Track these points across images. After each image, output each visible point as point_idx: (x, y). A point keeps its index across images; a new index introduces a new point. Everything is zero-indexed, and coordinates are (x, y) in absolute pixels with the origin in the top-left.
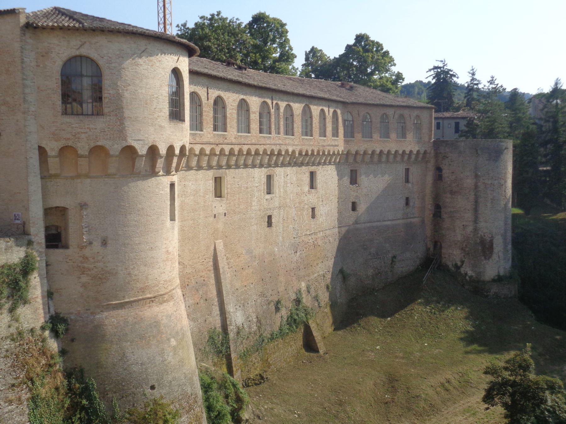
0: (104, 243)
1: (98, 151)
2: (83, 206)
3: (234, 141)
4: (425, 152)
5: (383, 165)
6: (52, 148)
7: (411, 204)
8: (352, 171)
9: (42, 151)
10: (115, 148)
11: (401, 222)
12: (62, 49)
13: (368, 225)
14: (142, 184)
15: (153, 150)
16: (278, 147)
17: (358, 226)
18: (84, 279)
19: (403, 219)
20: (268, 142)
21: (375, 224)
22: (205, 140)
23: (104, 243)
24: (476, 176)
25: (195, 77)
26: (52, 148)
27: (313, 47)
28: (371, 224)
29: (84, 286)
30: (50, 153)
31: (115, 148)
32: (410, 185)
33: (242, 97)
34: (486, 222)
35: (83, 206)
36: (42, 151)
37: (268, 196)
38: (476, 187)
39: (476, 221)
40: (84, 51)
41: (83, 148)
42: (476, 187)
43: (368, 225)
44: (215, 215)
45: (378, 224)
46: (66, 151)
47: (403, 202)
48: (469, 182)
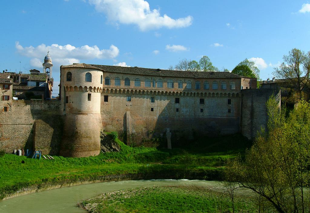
0: (73, 102)
1: (71, 87)
2: (70, 96)
3: (133, 88)
4: (237, 94)
6: (65, 86)
7: (231, 111)
9: (64, 87)
10: (73, 87)
11: (226, 117)
12: (67, 71)
13: (209, 117)
15: (81, 87)
18: (70, 108)
19: (227, 117)
20: (149, 89)
21: (211, 117)
22: (121, 87)
23: (73, 102)
24: (252, 102)
26: (65, 86)
28: (210, 117)
29: (70, 109)
30: (65, 87)
32: (231, 105)
35: (70, 96)
36: (64, 87)
38: (252, 105)
42: (252, 105)
43: (209, 117)
44: (127, 105)
45: (214, 117)
46: (67, 87)
47: (227, 111)
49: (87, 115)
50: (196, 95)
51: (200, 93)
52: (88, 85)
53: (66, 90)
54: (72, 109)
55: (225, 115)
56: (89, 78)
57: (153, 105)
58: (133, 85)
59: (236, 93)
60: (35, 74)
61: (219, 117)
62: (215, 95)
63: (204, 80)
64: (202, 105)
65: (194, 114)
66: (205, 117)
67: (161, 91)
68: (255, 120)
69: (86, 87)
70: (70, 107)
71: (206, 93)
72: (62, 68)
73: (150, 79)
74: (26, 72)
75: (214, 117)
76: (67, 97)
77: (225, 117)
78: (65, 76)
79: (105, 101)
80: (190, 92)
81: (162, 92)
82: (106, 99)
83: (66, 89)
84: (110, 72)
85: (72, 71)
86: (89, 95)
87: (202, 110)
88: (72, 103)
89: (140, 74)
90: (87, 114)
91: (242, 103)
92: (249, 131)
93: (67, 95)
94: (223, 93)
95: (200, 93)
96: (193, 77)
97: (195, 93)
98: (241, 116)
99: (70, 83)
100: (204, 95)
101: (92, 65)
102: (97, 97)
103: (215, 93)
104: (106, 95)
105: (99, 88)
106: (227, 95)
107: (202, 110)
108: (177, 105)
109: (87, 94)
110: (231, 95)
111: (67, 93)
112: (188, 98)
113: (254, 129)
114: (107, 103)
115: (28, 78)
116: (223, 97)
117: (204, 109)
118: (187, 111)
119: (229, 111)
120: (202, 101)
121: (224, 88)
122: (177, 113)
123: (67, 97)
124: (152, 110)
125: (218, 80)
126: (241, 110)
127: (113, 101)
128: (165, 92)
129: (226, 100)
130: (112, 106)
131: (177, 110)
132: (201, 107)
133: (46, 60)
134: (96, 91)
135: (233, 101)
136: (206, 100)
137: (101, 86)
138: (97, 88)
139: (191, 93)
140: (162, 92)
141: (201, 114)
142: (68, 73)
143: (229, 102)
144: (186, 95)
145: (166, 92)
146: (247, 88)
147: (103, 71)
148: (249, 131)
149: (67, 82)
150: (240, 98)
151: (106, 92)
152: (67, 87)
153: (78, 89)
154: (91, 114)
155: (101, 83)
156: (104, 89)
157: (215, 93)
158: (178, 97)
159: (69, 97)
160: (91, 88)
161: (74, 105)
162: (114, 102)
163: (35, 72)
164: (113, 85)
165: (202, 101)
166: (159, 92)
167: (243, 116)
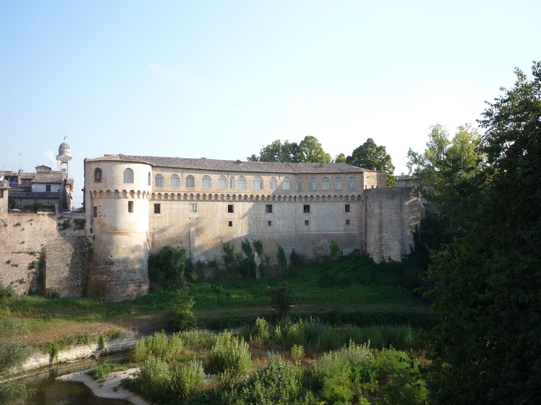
0: (104, 216)
1: (101, 192)
4: (359, 196)
5: (328, 203)
7: (351, 223)
8: (305, 206)
10: (105, 191)
11: (343, 232)
12: (94, 167)
14: (119, 200)
15: (117, 191)
16: (233, 194)
17: (309, 233)
21: (322, 233)
22: (180, 190)
23: (104, 216)
24: (381, 208)
25: (155, 168)
27: (370, 143)
31: (105, 191)
32: (349, 213)
33: (189, 174)
34: (387, 233)
37: (230, 214)
38: (381, 213)
39: (381, 231)
40: (98, 167)
41: (98, 191)
42: (381, 213)
45: (325, 232)
46: (95, 192)
48: (377, 211)
49: (127, 236)
50: (297, 199)
51: (303, 196)
52: (128, 188)
53: (94, 196)
54: (103, 225)
55: (342, 229)
56: (129, 176)
57: (232, 217)
58: (200, 187)
59: (356, 195)
60: (44, 173)
61: (333, 232)
62: (326, 199)
63: (309, 176)
64: (307, 214)
65: (295, 229)
66: (311, 233)
67: (243, 195)
68: (385, 234)
69: (125, 191)
70: (99, 223)
71: (312, 196)
72: (87, 163)
73: (226, 176)
74: (29, 169)
75: (325, 232)
76: (95, 208)
77: (341, 232)
78: (92, 175)
79: (156, 212)
80: (288, 196)
81: (246, 196)
82: (157, 209)
83: (93, 194)
84: (159, 164)
85: (102, 166)
86: (130, 204)
87: (307, 222)
88: (103, 216)
89: (210, 168)
90: (127, 234)
91: (366, 210)
92: (378, 251)
93: (95, 205)
94: (338, 196)
95: (303, 196)
96: (292, 172)
97: (295, 196)
98: (366, 230)
99: (99, 186)
100: (309, 199)
101: (134, 157)
102: (142, 206)
103: (326, 196)
104: (156, 202)
105: (146, 193)
106: (344, 199)
107: (307, 222)
108: (269, 217)
109: (126, 202)
110: (350, 199)
111: (95, 201)
112: (286, 204)
113: (384, 248)
114: (158, 215)
115: (32, 179)
116: (338, 201)
117: (309, 221)
118: (285, 224)
119: (348, 222)
120: (307, 209)
121: (340, 189)
122: (269, 228)
123: (95, 208)
124: (230, 224)
125: (330, 176)
126: (365, 221)
127: (168, 212)
128: (249, 197)
129: (342, 206)
130: (167, 219)
131: (270, 222)
132: (306, 216)
133: (62, 149)
134: (141, 196)
135: (354, 207)
136: (313, 207)
137: (150, 189)
138: (142, 192)
139: (290, 196)
140: (246, 196)
141: (306, 228)
142: (96, 170)
143: (347, 208)
144: (282, 199)
145: (252, 196)
146: (373, 186)
147: (152, 166)
148: (378, 251)
149: (95, 184)
150: (363, 201)
151: (156, 198)
152: (95, 192)
153: (113, 195)
154: (134, 234)
155: (149, 184)
156: (153, 194)
157: (326, 196)
158: (269, 204)
159: (98, 208)
160: (132, 192)
161: (106, 220)
162: (170, 214)
163: (44, 169)
164: (168, 188)
165: (307, 209)
166: (240, 196)
167: (368, 230)
